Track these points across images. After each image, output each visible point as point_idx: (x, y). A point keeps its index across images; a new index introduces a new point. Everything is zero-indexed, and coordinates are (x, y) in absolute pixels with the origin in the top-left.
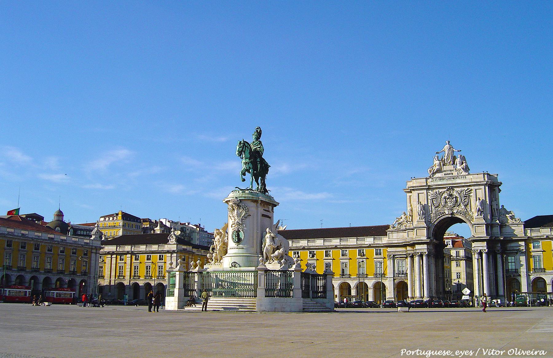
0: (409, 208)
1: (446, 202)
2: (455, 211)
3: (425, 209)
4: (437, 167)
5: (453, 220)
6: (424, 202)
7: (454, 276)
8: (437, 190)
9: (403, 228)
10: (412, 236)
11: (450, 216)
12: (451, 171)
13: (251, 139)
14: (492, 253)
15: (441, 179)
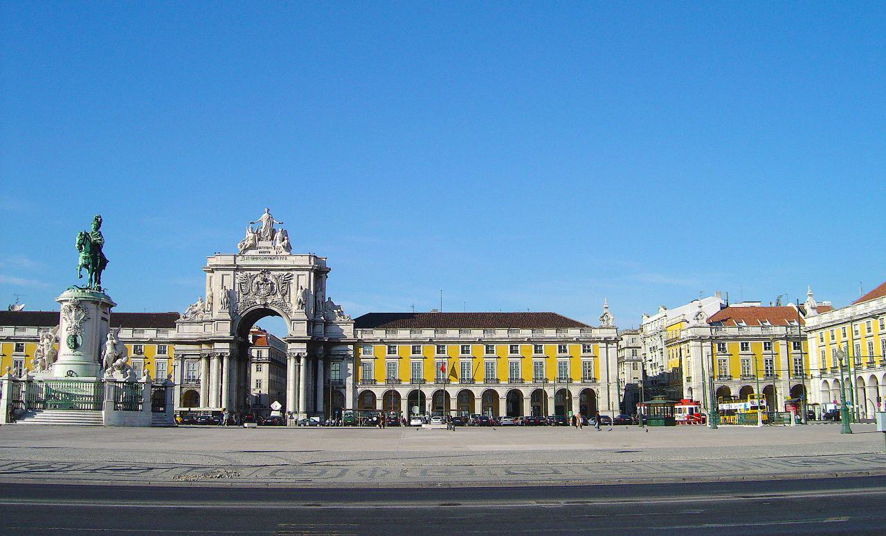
0: (208, 293)
1: (258, 289)
2: (269, 302)
3: (230, 295)
4: (250, 242)
5: (265, 312)
6: (229, 287)
7: (253, 385)
8: (248, 272)
9: (198, 318)
10: (210, 331)
11: (262, 307)
12: (268, 248)
13: (91, 229)
14: (312, 359)
15: (254, 258)
